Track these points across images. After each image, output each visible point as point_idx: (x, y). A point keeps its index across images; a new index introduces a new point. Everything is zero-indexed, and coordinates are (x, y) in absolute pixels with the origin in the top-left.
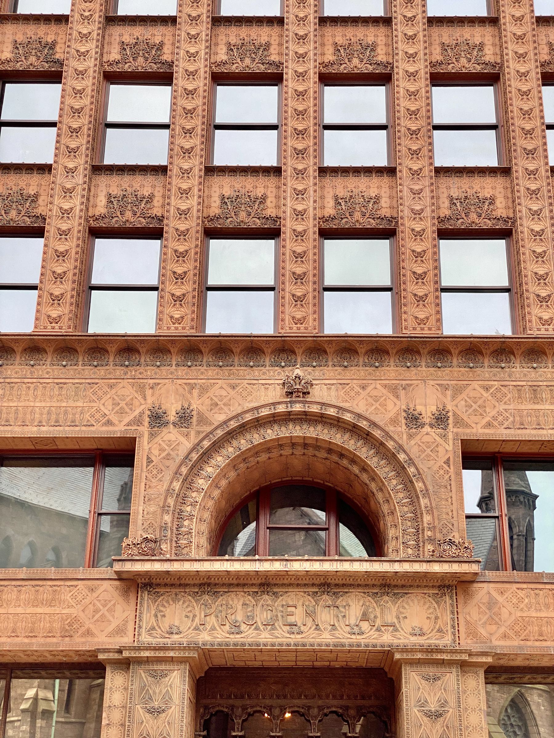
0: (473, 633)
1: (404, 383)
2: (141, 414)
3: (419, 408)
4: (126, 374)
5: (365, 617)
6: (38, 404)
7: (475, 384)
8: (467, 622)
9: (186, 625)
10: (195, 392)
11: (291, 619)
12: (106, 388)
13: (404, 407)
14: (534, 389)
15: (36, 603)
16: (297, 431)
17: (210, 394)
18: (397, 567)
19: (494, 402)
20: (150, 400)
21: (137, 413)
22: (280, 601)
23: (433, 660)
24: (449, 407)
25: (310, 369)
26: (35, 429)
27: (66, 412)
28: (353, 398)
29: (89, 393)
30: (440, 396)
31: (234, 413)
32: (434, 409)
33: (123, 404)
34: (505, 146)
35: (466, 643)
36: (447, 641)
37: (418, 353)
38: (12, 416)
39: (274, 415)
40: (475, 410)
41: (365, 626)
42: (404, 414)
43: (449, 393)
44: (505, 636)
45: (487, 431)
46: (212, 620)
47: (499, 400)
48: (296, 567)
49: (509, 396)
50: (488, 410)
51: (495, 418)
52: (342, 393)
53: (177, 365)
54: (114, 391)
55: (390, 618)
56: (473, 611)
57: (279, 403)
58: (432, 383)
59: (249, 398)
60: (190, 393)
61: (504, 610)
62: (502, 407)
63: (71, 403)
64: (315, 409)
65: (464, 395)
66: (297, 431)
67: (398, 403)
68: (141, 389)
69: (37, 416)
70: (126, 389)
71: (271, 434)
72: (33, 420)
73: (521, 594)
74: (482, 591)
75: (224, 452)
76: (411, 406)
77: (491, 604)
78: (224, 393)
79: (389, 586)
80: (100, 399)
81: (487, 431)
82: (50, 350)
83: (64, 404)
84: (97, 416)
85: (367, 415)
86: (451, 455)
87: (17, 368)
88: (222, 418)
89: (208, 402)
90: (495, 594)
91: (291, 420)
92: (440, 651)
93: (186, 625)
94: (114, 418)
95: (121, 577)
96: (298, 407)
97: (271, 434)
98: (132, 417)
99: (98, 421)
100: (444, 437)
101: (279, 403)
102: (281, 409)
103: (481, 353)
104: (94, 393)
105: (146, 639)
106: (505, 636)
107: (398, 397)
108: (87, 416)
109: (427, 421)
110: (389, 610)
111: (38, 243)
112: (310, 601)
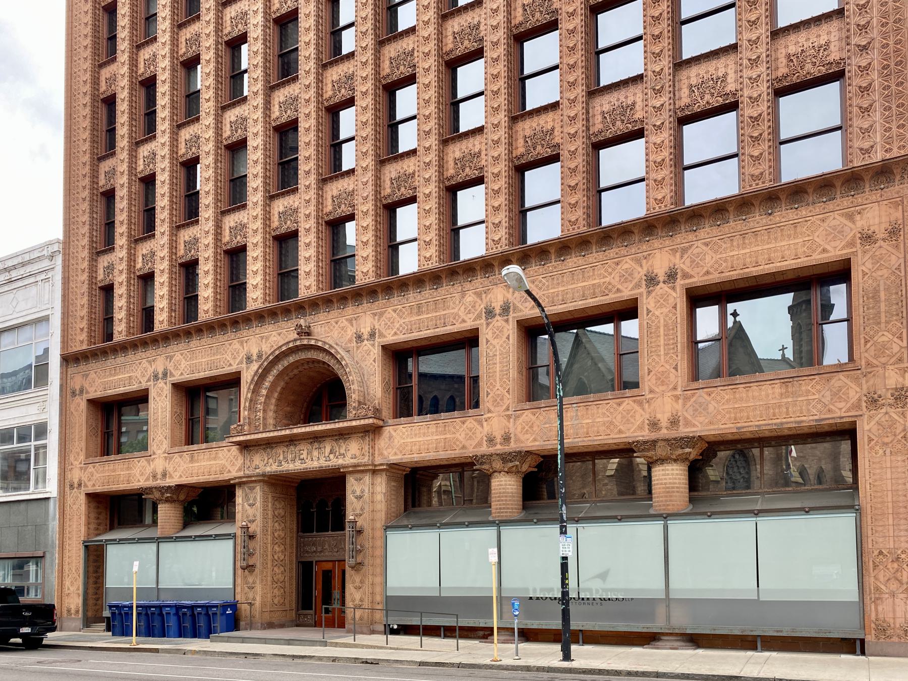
0: (381, 454)
5: (331, 452)
8: (379, 449)
9: (261, 464)
11: (302, 457)
15: (209, 459)
16: (303, 356)
18: (354, 423)
22: (298, 448)
23: (358, 470)
35: (378, 461)
36: (365, 460)
41: (332, 456)
43: (376, 317)
44: (396, 454)
45: (394, 338)
46: (271, 460)
47: (401, 317)
48: (295, 431)
51: (398, 329)
55: (342, 451)
56: (382, 442)
61: (396, 441)
63: (216, 357)
65: (384, 318)
66: (303, 356)
71: (292, 359)
73: (404, 430)
74: (387, 430)
75: (272, 373)
77: (391, 437)
79: (342, 435)
81: (394, 338)
86: (376, 356)
90: (392, 432)
91: (298, 350)
92: (359, 466)
93: (261, 464)
95: (238, 443)
97: (292, 359)
100: (373, 345)
105: (247, 472)
106: (396, 454)
109: (366, 337)
110: (343, 447)
112: (310, 447)
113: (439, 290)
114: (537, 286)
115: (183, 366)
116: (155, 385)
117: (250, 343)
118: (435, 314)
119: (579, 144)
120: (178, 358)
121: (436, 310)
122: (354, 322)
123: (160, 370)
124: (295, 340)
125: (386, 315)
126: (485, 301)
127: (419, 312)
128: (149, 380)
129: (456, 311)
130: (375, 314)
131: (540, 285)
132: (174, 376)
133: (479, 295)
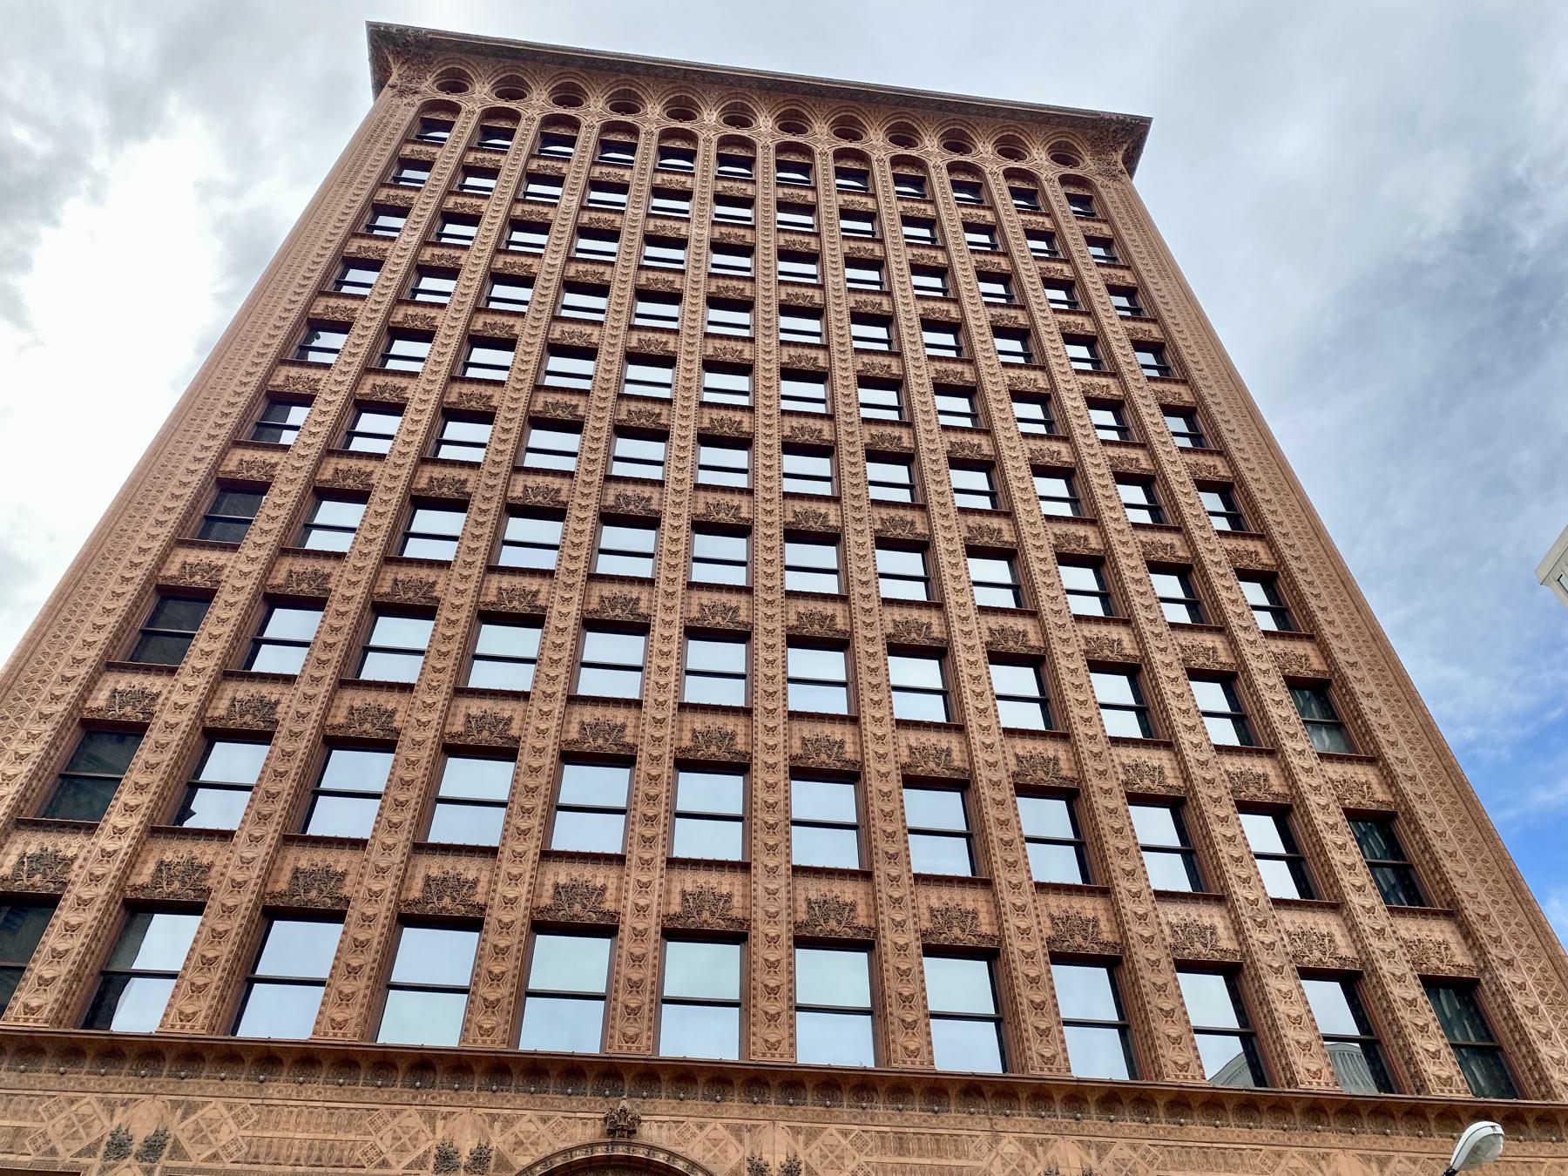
1: (749, 1123)
2: (426, 1154)
3: (767, 1157)
4: (414, 1098)
6: (299, 1135)
7: (832, 1128)
10: (497, 1125)
12: (387, 1117)
13: (748, 1155)
14: (900, 1138)
17: (516, 1129)
19: (854, 1152)
20: (440, 1134)
21: (421, 1152)
24: (801, 1157)
25: (639, 1101)
26: (289, 1169)
27: (332, 1148)
28: (687, 1141)
29: (366, 1122)
30: (791, 1142)
31: (542, 1156)
32: (783, 1158)
33: (405, 1139)
34: (854, 699)
37: (767, 1085)
38: (263, 1150)
39: (589, 1160)
40: (832, 1162)
42: (747, 1165)
43: (801, 1138)
47: (860, 1150)
49: (872, 1144)
50: (846, 1162)
52: (675, 1133)
53: (479, 1089)
54: (397, 1120)
57: (598, 1144)
58: (782, 1124)
59: (563, 1136)
60: (491, 1126)
62: (862, 1159)
64: (641, 1154)
65: (818, 1142)
67: (741, 1149)
68: (431, 1119)
69: (295, 1151)
70: (412, 1118)
72: (289, 1157)
76: (757, 1154)
78: (532, 1128)
80: (377, 1130)
82: (288, 1061)
83: (331, 1137)
84: (371, 1154)
85: (702, 1163)
87: (281, 1085)
88: (526, 1161)
89: (512, 1139)
94: (391, 1157)
96: (620, 1151)
98: (414, 1156)
99: (370, 1161)
101: (598, 1144)
102: (600, 1152)
103: (839, 1088)
104: (372, 1123)
107: (741, 1141)
108: (358, 1154)
111: (336, 929)
113: (943, 1116)
114: (1144, 1157)
115: (224, 1137)
116: (103, 1169)
117: (453, 1123)
118: (937, 1162)
119: (383, 910)
120: (214, 1114)
121: (939, 1152)
122: (746, 1136)
123: (141, 1132)
124: (592, 1146)
125: (824, 1136)
126: (1043, 1161)
127: (902, 1149)
128: (90, 1151)
129: (984, 1164)
130: (796, 1131)
131: (1149, 1157)
132: (186, 1157)
133: (1029, 1145)
